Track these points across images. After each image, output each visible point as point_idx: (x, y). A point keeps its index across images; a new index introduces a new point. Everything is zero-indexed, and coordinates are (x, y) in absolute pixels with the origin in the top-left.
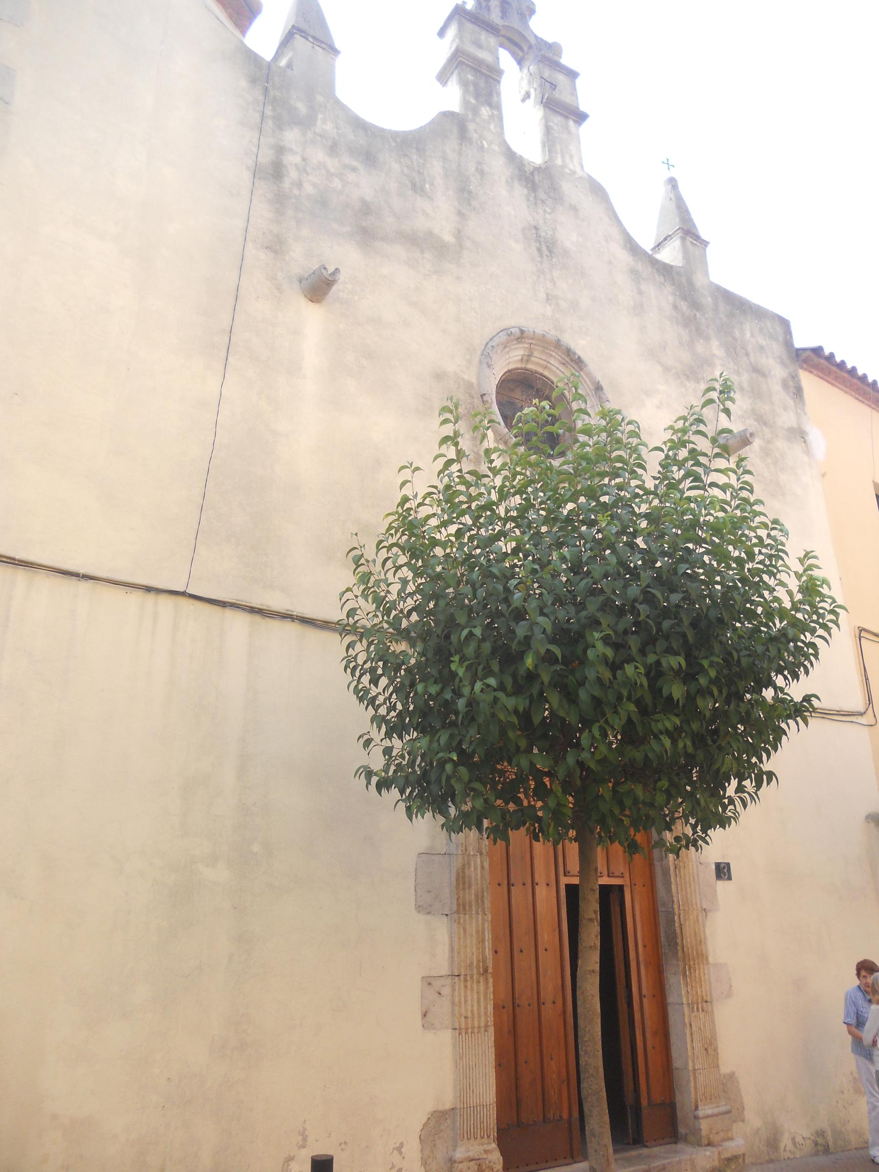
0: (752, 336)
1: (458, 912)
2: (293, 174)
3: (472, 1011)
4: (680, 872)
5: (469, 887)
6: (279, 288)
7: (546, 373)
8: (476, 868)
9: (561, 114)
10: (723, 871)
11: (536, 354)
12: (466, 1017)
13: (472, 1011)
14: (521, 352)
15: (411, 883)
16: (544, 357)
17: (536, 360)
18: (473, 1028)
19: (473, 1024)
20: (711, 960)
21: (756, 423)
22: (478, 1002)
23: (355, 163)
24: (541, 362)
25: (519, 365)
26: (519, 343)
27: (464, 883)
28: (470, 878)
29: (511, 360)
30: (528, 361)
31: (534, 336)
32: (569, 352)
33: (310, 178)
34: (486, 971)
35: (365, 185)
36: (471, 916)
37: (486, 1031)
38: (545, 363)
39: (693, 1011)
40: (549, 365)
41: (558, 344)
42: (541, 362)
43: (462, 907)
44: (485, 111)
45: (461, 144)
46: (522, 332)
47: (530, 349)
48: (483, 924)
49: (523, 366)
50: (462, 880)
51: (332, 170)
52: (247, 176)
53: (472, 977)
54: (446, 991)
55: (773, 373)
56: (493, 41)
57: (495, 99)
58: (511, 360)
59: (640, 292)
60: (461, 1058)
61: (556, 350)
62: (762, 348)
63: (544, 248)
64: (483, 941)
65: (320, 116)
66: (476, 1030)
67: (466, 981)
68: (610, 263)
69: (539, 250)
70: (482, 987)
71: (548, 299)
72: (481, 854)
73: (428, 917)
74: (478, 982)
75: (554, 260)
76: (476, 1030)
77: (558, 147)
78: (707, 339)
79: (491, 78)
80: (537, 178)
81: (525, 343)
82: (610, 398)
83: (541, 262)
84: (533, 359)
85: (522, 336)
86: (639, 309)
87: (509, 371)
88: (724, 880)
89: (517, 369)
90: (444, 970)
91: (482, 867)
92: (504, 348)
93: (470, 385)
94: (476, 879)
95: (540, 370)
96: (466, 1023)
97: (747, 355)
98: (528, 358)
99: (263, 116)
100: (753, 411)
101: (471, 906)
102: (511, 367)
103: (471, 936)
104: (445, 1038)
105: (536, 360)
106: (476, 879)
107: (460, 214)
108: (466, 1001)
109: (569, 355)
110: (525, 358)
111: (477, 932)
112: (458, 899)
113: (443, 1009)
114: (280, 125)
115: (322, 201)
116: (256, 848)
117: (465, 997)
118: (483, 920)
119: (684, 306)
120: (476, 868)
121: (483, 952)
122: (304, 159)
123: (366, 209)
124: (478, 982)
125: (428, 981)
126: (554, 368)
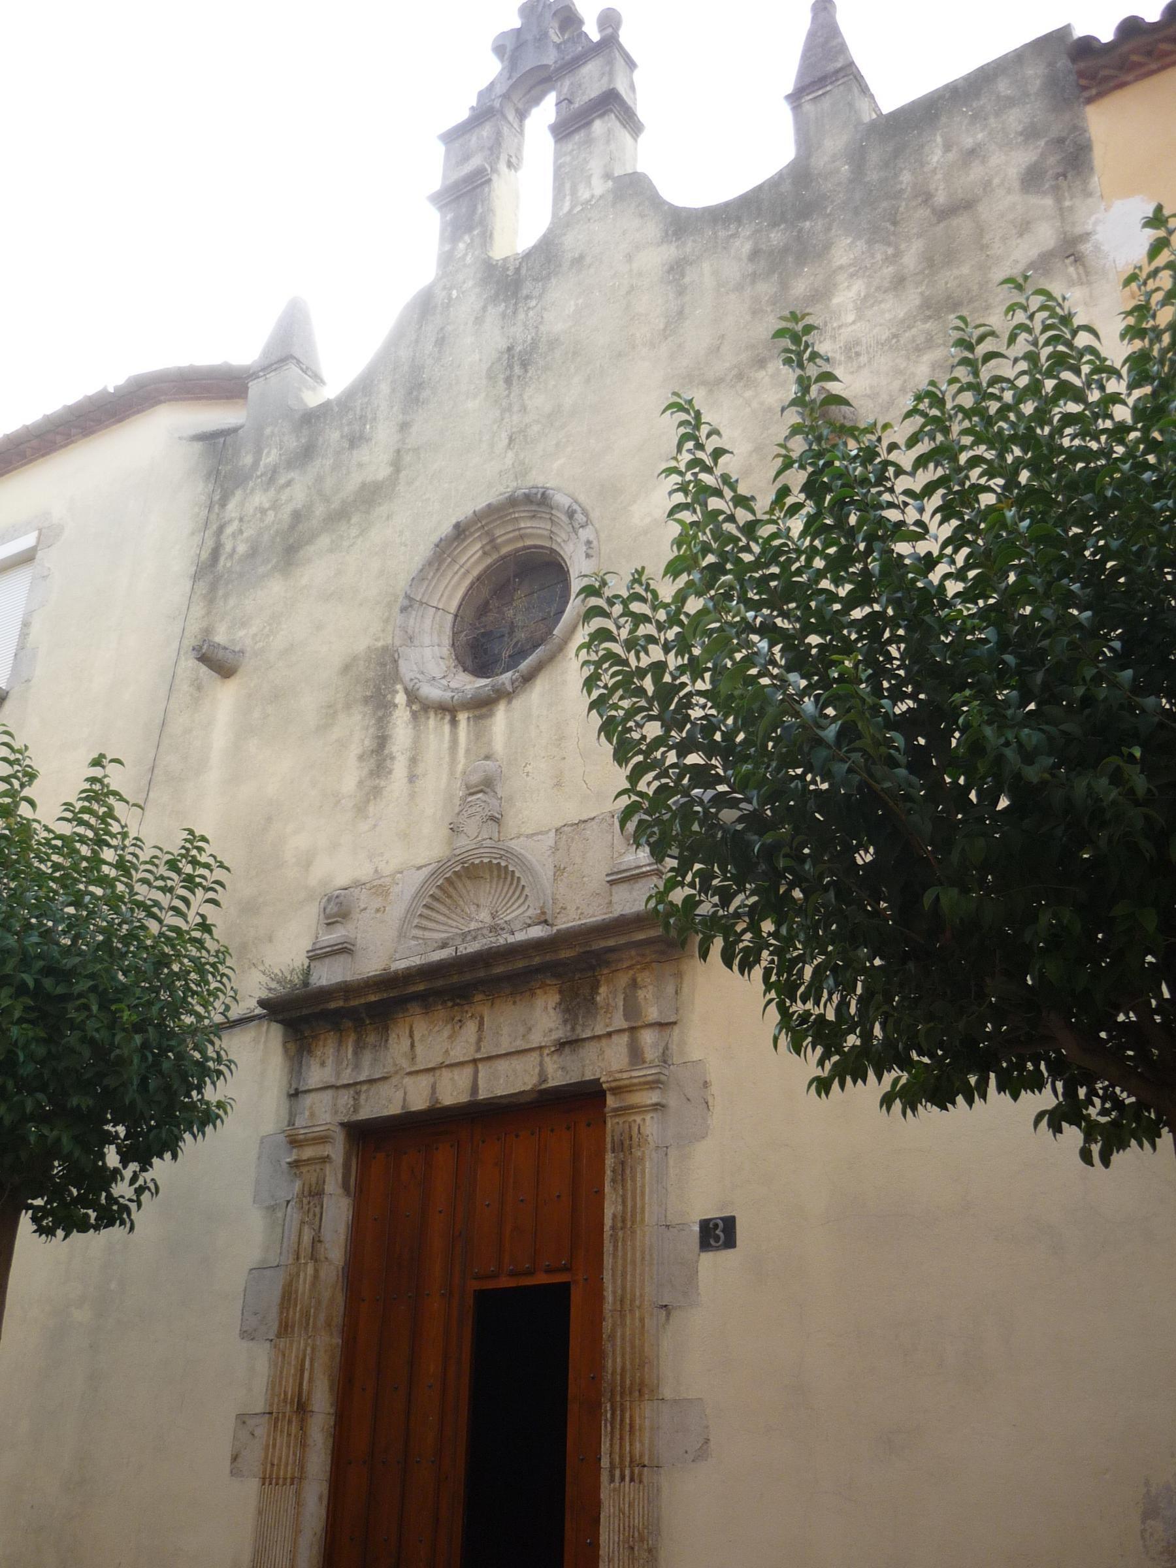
0: (947, 148)
1: (279, 1336)
2: (228, 547)
3: (280, 1458)
4: (615, 1247)
5: (296, 1305)
6: (199, 688)
7: (529, 543)
8: (305, 1280)
9: (578, 130)
10: (718, 1233)
11: (498, 533)
12: (273, 1465)
13: (280, 1458)
14: (478, 546)
15: (239, 1304)
16: (510, 528)
17: (504, 538)
18: (278, 1478)
19: (286, 1472)
20: (667, 1392)
21: (928, 326)
22: (288, 1446)
23: (291, 475)
24: (511, 535)
25: (489, 561)
26: (464, 540)
27: (289, 1300)
28: (297, 1291)
29: (466, 567)
30: (496, 548)
31: (478, 517)
32: (528, 499)
33: (245, 535)
34: (302, 1408)
35: (298, 493)
36: (291, 1344)
37: (292, 1483)
38: (517, 533)
39: (612, 1480)
40: (522, 532)
41: (512, 502)
42: (511, 535)
43: (285, 1329)
44: (461, 246)
45: (420, 327)
46: (457, 526)
47: (487, 533)
48: (305, 1350)
49: (495, 556)
50: (288, 1297)
51: (267, 505)
52: (188, 584)
53: (284, 1416)
54: (261, 1431)
55: (996, 181)
56: (486, 131)
57: (480, 210)
58: (466, 567)
59: (681, 292)
60: (260, 1513)
61: (516, 509)
62: (972, 154)
63: (517, 370)
64: (302, 1371)
65: (265, 451)
66: (281, 1482)
67: (277, 1419)
68: (632, 289)
69: (508, 381)
70: (294, 1429)
71: (511, 440)
72: (316, 1261)
73: (251, 1344)
74: (290, 1422)
75: (529, 375)
76: (281, 1482)
77: (568, 186)
78: (827, 247)
79: (477, 187)
80: (523, 271)
81: (471, 534)
82: (594, 515)
83: (508, 396)
84: (499, 540)
85: (461, 532)
86: (675, 320)
87: (478, 578)
88: (718, 1248)
89: (489, 567)
90: (260, 1406)
91: (316, 1276)
92: (440, 565)
93: (385, 649)
94: (303, 1293)
95: (520, 545)
96: (272, 1471)
97: (928, 198)
98: (493, 544)
99: (210, 508)
100: (926, 304)
101: (293, 1327)
102: (475, 573)
103: (289, 1363)
104: (251, 1487)
105: (504, 538)
106: (303, 1293)
107: (404, 427)
108: (274, 1446)
109: (531, 502)
110: (488, 548)
111: (297, 1357)
112: (281, 1323)
113: (254, 1455)
114: (223, 504)
115: (253, 553)
116: (113, 1286)
117: (275, 1439)
118: (306, 1345)
119: (777, 237)
120: (305, 1280)
121: (301, 1384)
122: (241, 520)
123: (297, 516)
124: (290, 1422)
125: (242, 1419)
126: (528, 531)
